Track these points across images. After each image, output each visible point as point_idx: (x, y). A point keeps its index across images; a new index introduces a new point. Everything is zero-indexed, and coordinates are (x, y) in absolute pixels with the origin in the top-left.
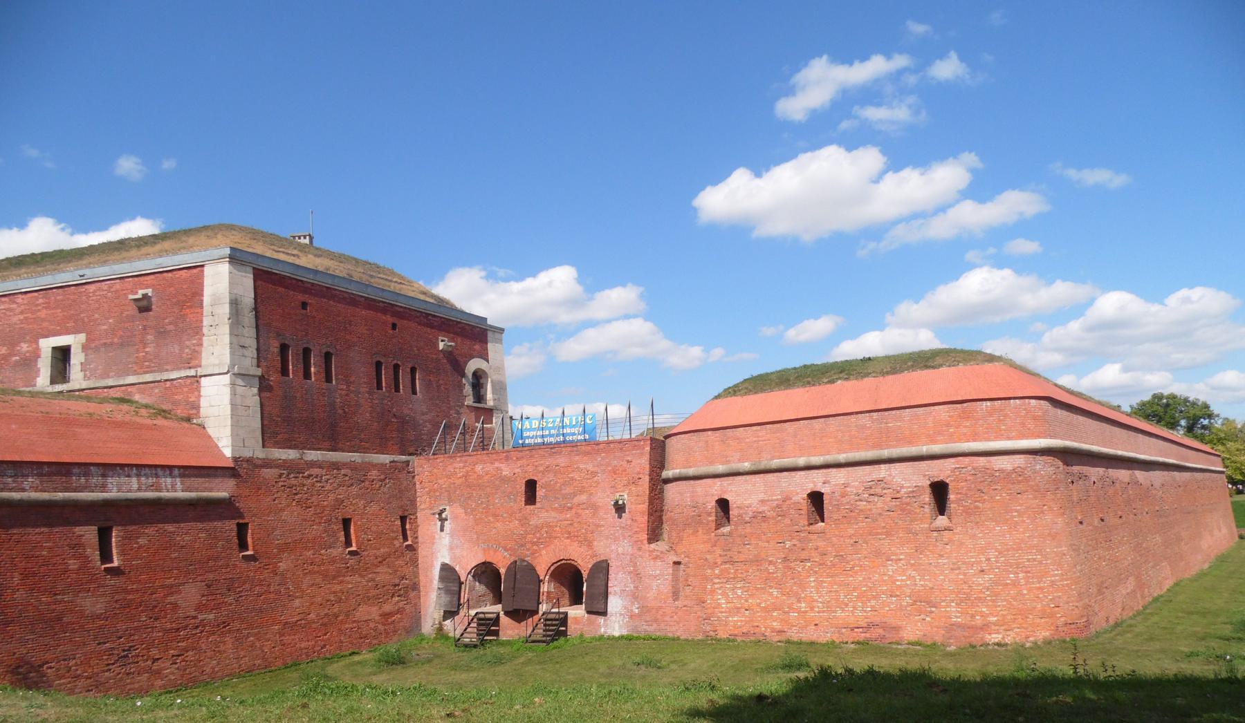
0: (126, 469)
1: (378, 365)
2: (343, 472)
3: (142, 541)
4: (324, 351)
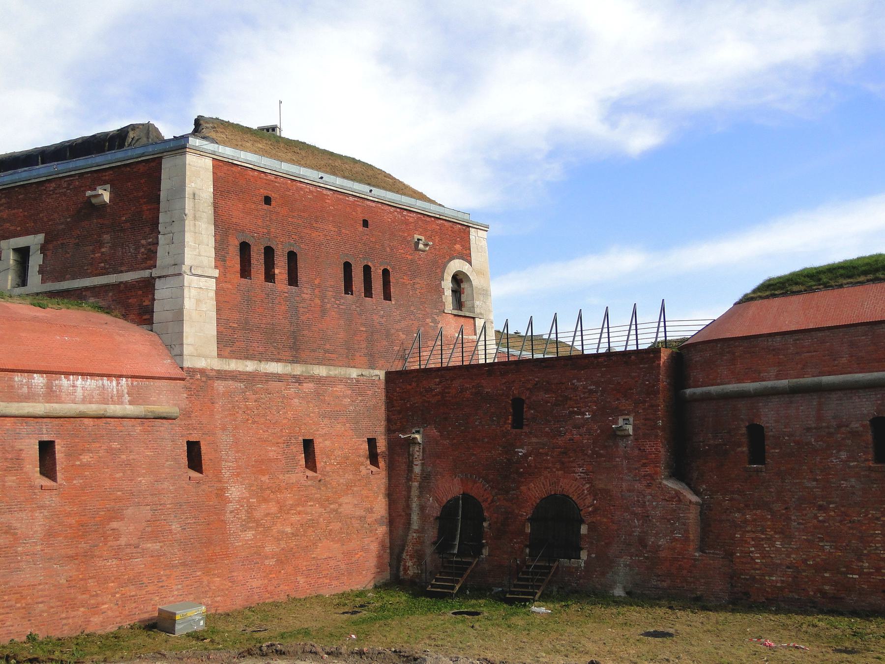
0: (71, 377)
1: (347, 267)
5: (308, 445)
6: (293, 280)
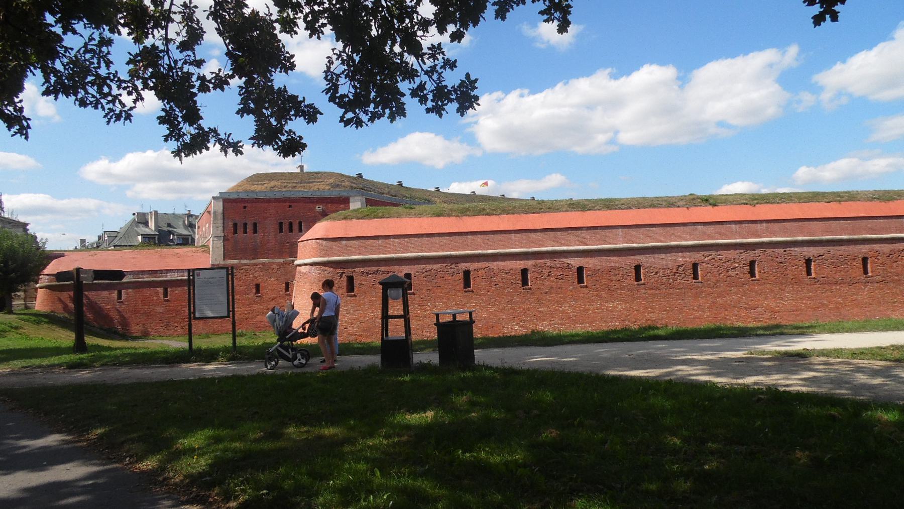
1: (281, 224)
2: (258, 267)
3: (177, 292)
4: (253, 222)
6: (255, 231)
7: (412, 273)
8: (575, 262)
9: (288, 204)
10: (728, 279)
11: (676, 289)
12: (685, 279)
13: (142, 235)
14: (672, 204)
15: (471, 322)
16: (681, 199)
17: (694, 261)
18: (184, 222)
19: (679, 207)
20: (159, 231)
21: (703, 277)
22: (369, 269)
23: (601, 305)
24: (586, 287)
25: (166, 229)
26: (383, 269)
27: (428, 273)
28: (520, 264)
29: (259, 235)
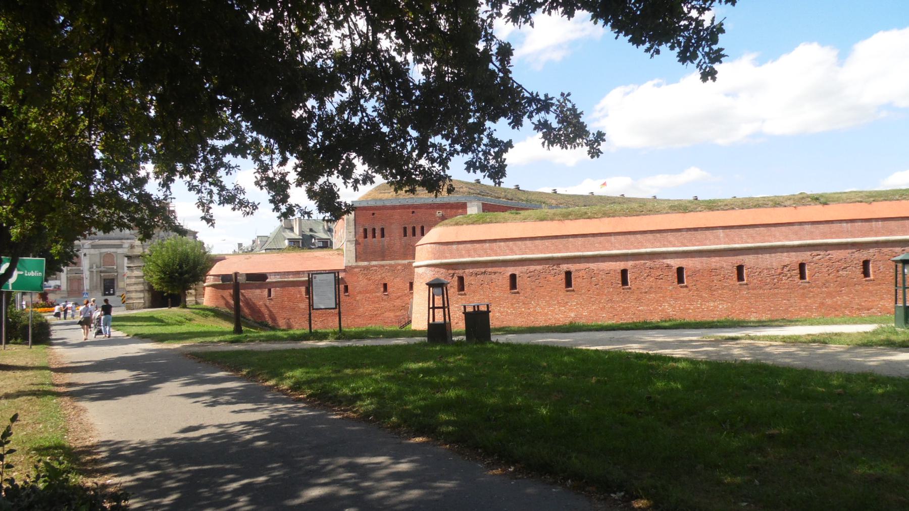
1: (405, 229)
5: (385, 286)
6: (383, 236)
7: (517, 273)
8: (675, 263)
9: (411, 210)
10: (838, 279)
11: (781, 289)
12: (791, 279)
13: (288, 239)
14: (779, 204)
15: (488, 312)
16: (789, 198)
17: (800, 260)
18: (324, 227)
19: (785, 206)
20: (303, 235)
21: (812, 276)
22: (478, 270)
23: (701, 304)
24: (686, 287)
25: (309, 233)
26: (490, 270)
27: (532, 274)
28: (621, 265)
29: (386, 239)
